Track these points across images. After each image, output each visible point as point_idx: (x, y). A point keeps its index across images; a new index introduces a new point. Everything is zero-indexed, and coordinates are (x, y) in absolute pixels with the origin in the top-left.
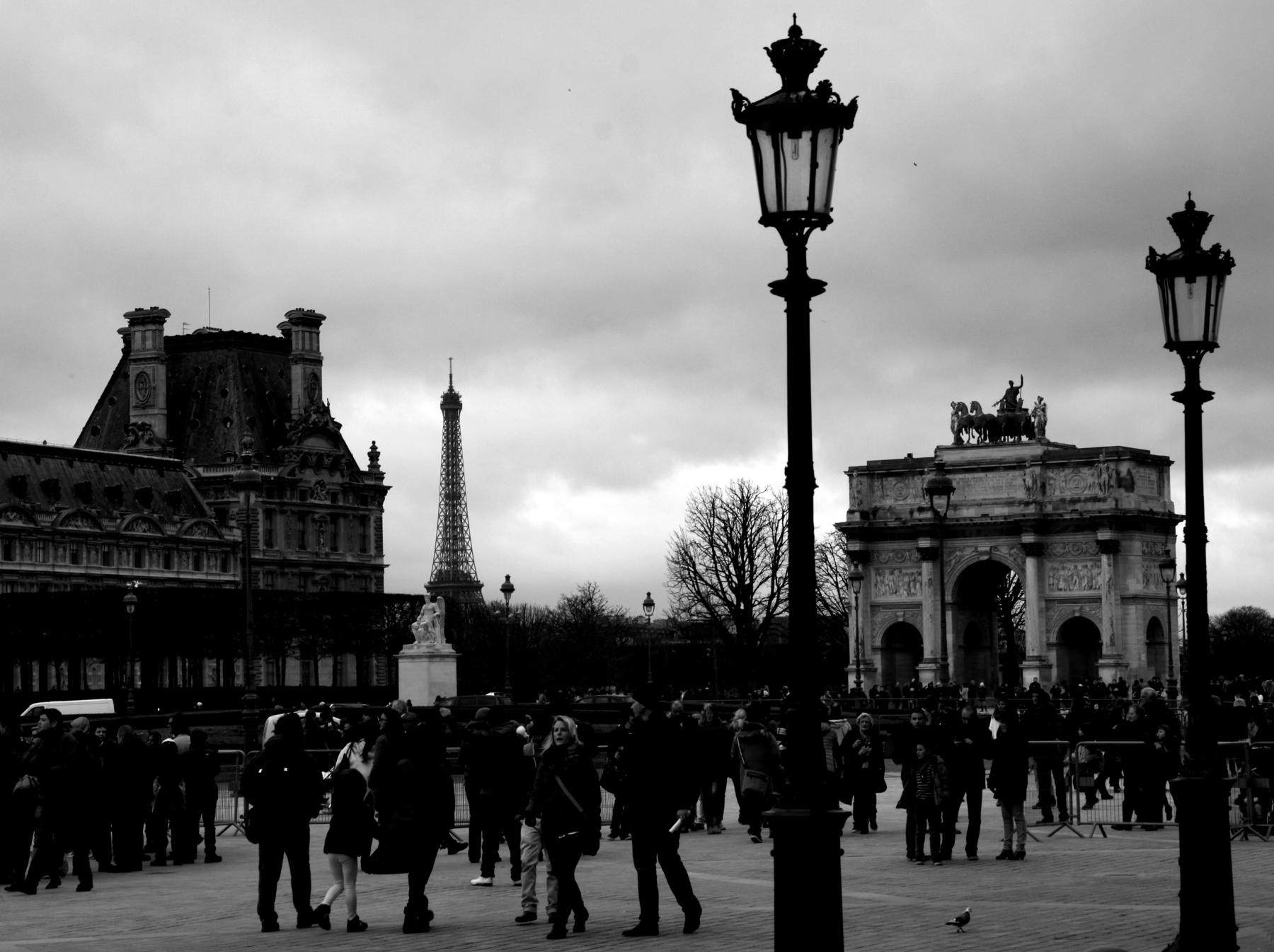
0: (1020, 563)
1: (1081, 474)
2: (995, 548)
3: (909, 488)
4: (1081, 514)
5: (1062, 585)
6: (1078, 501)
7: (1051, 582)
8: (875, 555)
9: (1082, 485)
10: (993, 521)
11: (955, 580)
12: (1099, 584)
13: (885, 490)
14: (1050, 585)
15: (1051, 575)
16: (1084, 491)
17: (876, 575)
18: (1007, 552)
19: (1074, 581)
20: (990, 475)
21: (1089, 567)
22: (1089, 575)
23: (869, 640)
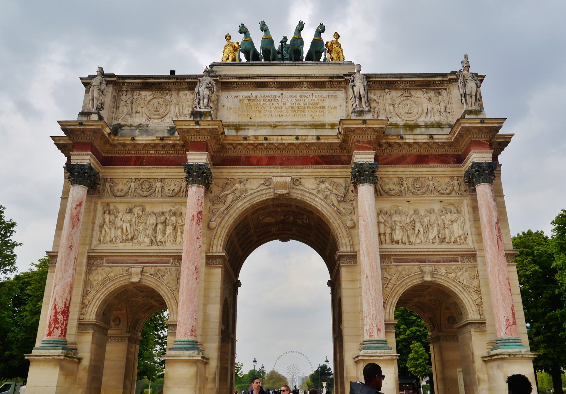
0: (336, 203)
1: (413, 98)
2: (296, 181)
3: (170, 105)
4: (431, 137)
5: (398, 235)
6: (417, 126)
7: (382, 231)
8: (108, 185)
9: (416, 110)
10: (300, 141)
11: (231, 221)
12: (456, 235)
13: (133, 106)
14: (380, 235)
15: (383, 221)
16: (419, 118)
17: (104, 212)
18: (314, 186)
19: (417, 231)
20: (287, 93)
21: (436, 211)
22: (440, 222)
23: (77, 309)
